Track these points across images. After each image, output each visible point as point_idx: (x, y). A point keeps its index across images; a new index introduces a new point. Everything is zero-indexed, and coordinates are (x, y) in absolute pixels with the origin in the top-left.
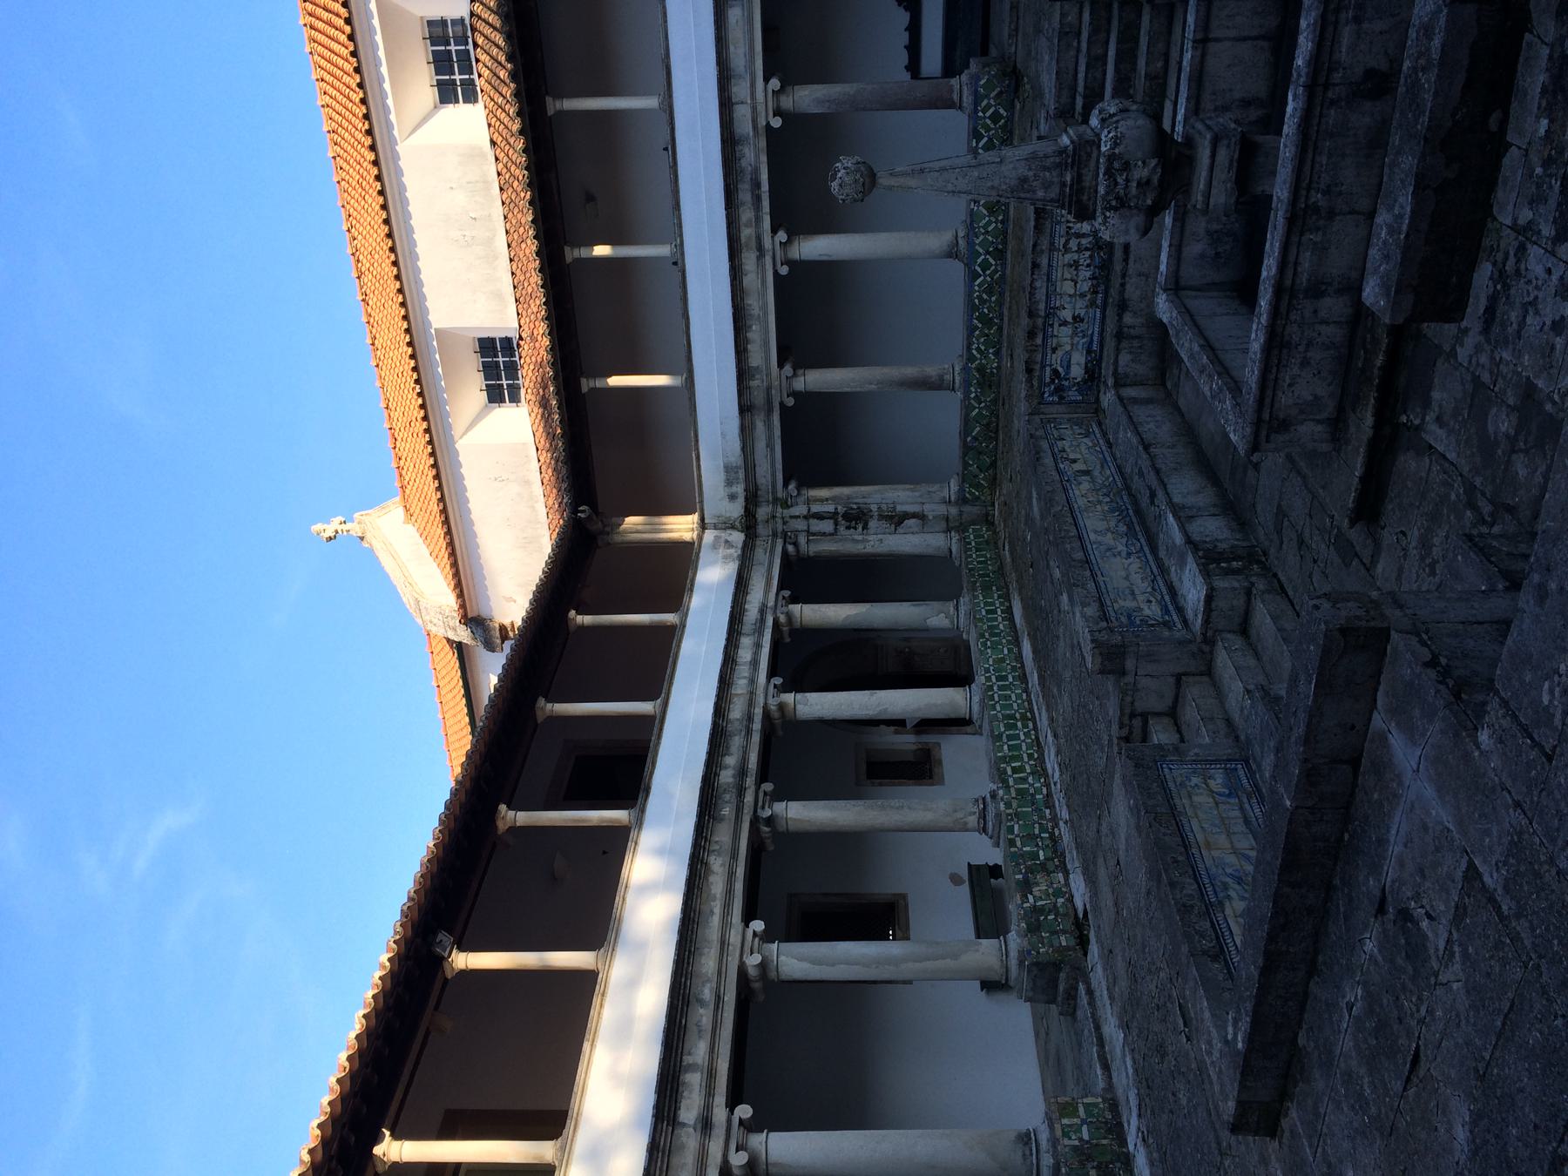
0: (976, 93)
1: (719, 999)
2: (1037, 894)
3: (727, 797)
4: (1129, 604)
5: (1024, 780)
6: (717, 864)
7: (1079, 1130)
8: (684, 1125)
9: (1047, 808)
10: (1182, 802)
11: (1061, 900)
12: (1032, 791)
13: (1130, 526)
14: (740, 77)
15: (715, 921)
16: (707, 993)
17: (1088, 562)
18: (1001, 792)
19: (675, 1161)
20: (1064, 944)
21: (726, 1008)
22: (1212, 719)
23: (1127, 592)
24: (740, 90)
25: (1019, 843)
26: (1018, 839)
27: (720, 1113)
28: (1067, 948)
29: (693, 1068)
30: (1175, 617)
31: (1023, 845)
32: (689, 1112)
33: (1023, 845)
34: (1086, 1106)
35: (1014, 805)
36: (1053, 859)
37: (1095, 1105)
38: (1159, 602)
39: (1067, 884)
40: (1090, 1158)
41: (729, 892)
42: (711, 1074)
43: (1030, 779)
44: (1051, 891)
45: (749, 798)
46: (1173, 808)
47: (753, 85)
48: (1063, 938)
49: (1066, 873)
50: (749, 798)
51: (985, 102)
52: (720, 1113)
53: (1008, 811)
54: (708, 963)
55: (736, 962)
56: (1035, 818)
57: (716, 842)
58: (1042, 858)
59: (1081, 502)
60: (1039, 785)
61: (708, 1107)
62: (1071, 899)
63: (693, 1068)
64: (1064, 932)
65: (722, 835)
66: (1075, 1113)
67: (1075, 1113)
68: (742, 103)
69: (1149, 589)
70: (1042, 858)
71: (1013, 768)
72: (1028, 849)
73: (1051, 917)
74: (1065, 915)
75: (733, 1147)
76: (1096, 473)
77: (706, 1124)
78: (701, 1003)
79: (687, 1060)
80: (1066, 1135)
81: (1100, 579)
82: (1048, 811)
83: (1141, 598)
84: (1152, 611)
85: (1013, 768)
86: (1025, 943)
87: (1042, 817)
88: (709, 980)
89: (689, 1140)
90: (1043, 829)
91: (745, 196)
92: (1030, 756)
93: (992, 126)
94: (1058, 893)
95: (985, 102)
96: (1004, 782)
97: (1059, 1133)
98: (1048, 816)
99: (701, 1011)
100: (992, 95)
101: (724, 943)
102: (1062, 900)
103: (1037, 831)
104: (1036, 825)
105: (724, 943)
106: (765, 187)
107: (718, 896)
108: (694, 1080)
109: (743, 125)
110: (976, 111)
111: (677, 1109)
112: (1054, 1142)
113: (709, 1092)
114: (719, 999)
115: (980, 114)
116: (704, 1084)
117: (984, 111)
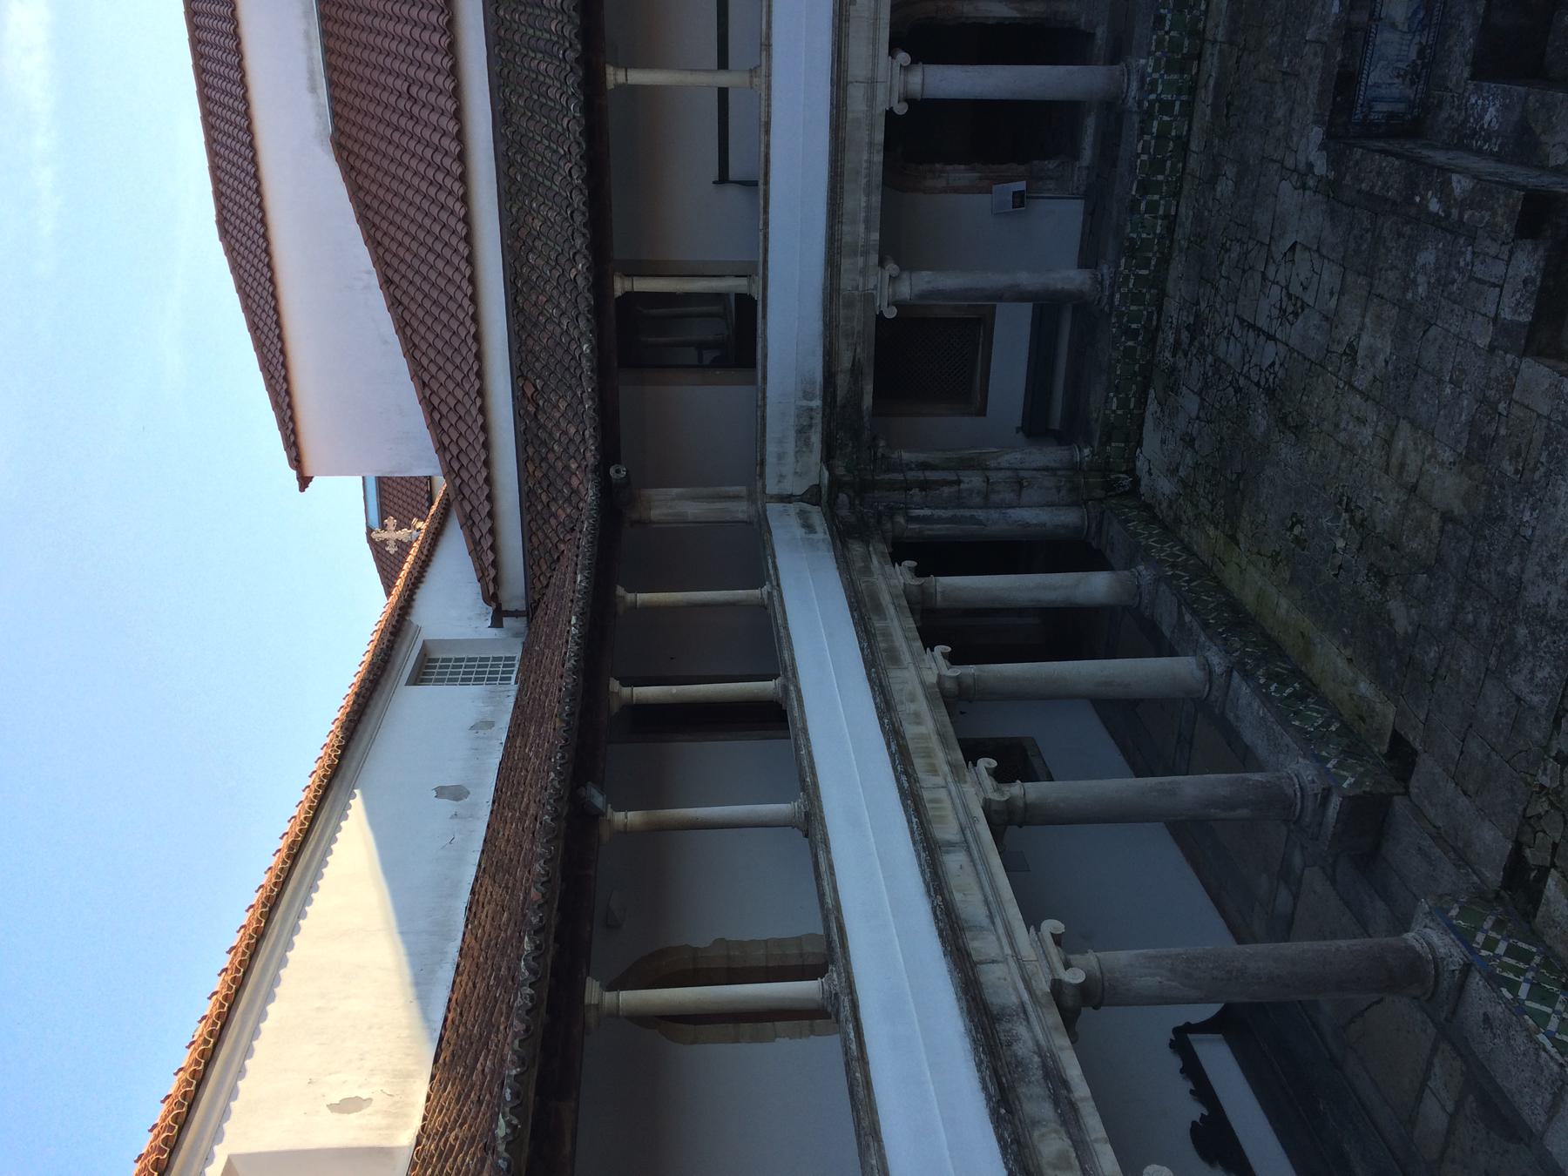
0: (1452, 928)
14: (982, 928)
24: (983, 945)
47: (1010, 935)
51: (1480, 938)
68: (993, 962)
91: (1036, 1104)
93: (1522, 965)
95: (1480, 938)
100: (1487, 925)
106: (1081, 1090)
109: (1002, 984)
110: (1472, 950)
115: (1484, 953)
117: (1490, 944)
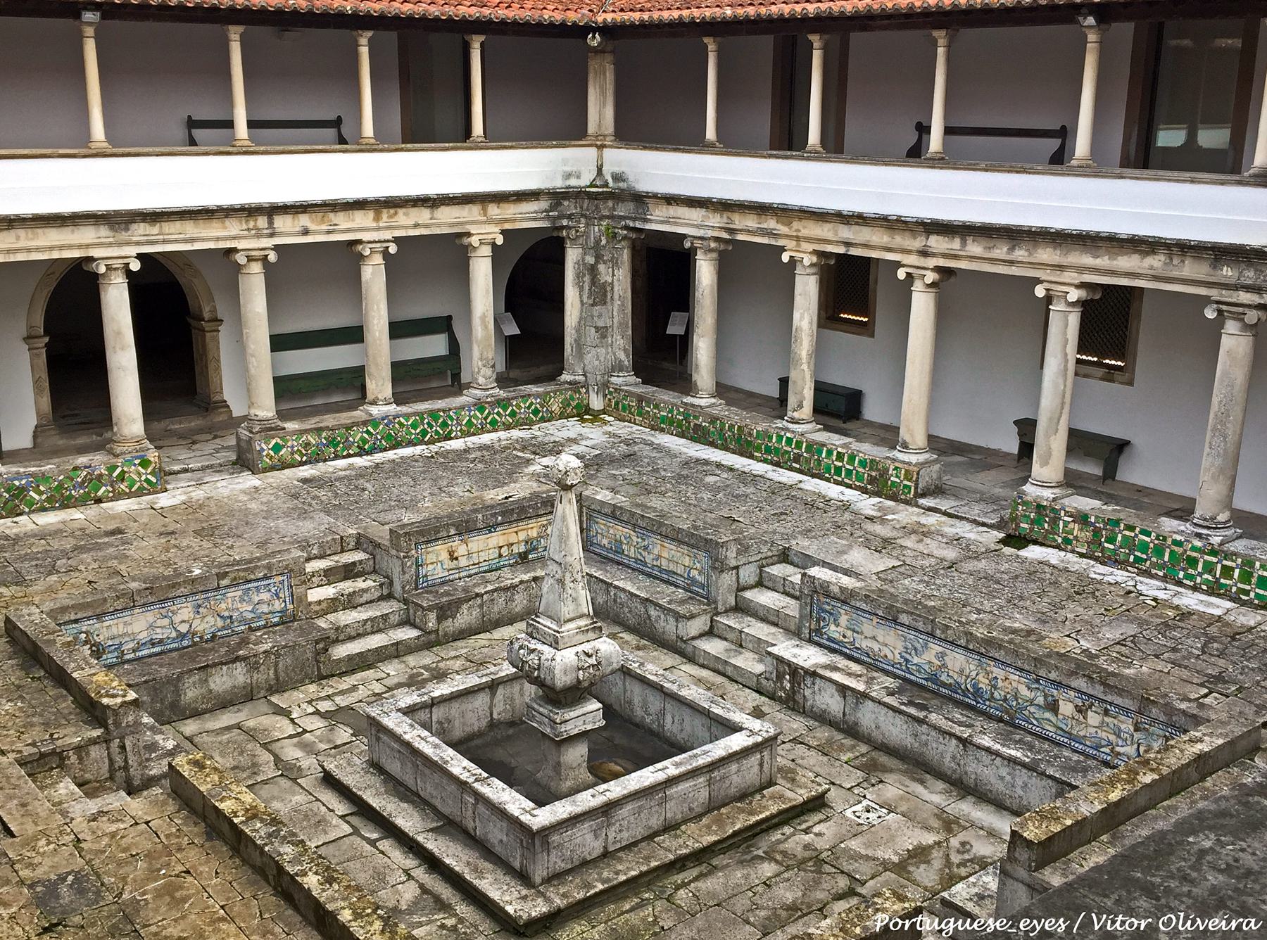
1: (1012, 262)
2: (1071, 525)
3: (1250, 274)
4: (843, 620)
5: (1209, 568)
6: (1156, 262)
7: (897, 477)
8: (927, 239)
9: (1165, 576)
10: (685, 549)
11: (1060, 540)
12: (1191, 571)
13: (944, 685)
15: (1087, 260)
16: (1020, 254)
17: (895, 621)
18: (1198, 543)
19: (907, 233)
20: (1022, 525)
21: (1005, 268)
22: (778, 616)
23: (857, 629)
25: (1127, 533)
26: (1132, 534)
27: (932, 262)
28: (1018, 526)
29: (964, 243)
30: (825, 642)
31: (1124, 536)
32: (937, 243)
33: (1124, 536)
34: (910, 487)
35: (1176, 549)
36: (1102, 552)
37: (909, 492)
38: (842, 642)
39: (1073, 551)
40: (882, 476)
41: (1114, 273)
42: (956, 257)
43: (1210, 578)
44: (1071, 537)
45: (1245, 297)
46: (683, 543)
48: (1026, 526)
49: (1082, 555)
50: (1245, 297)
52: (932, 262)
53: (1169, 541)
54: (1046, 254)
55: (1043, 278)
56: (1154, 559)
57: (1183, 262)
58: (1106, 545)
59: (998, 672)
60: (1199, 580)
61: (934, 255)
62: (1058, 547)
63: (964, 243)
64: (1032, 530)
65: (1190, 268)
66: (906, 478)
67: (906, 478)
69: (857, 645)
70: (1106, 545)
71: (1232, 569)
72: (1119, 537)
73: (1046, 525)
74: (1045, 537)
75: (909, 270)
76: (1047, 715)
77: (924, 253)
78: (1012, 249)
79: (970, 240)
80: (896, 468)
81: (875, 620)
82: (1161, 574)
83: (849, 633)
84: (833, 631)
85: (1232, 569)
86: (1029, 498)
87: (1154, 565)
88: (1030, 254)
89: (918, 243)
90: (1138, 560)
92: (1247, 593)
94: (1067, 541)
96: (1213, 552)
97: (897, 465)
98: (1154, 571)
99: (1005, 249)
101: (1060, 267)
102: (1060, 540)
103: (1136, 553)
104: (1144, 556)
105: (1060, 267)
107: (1115, 262)
108: (956, 244)
111: (938, 234)
112: (894, 460)
113: (944, 256)
114: (1012, 262)
116: (952, 252)
